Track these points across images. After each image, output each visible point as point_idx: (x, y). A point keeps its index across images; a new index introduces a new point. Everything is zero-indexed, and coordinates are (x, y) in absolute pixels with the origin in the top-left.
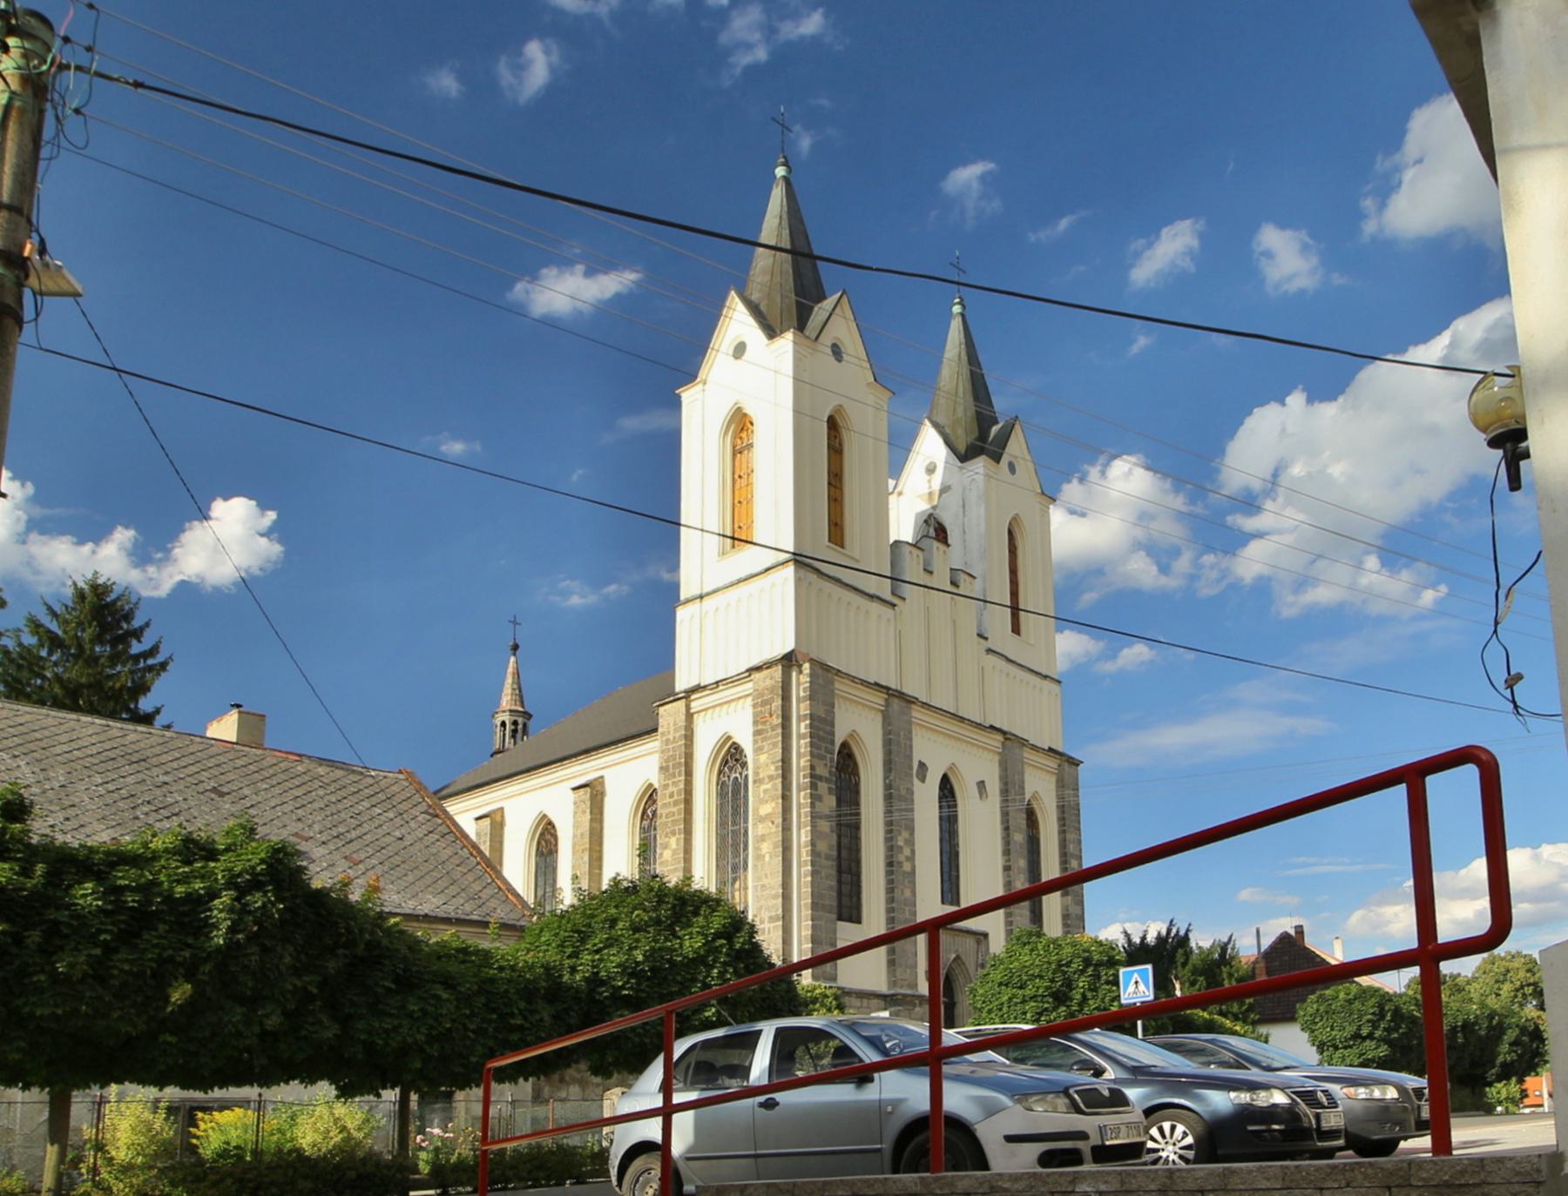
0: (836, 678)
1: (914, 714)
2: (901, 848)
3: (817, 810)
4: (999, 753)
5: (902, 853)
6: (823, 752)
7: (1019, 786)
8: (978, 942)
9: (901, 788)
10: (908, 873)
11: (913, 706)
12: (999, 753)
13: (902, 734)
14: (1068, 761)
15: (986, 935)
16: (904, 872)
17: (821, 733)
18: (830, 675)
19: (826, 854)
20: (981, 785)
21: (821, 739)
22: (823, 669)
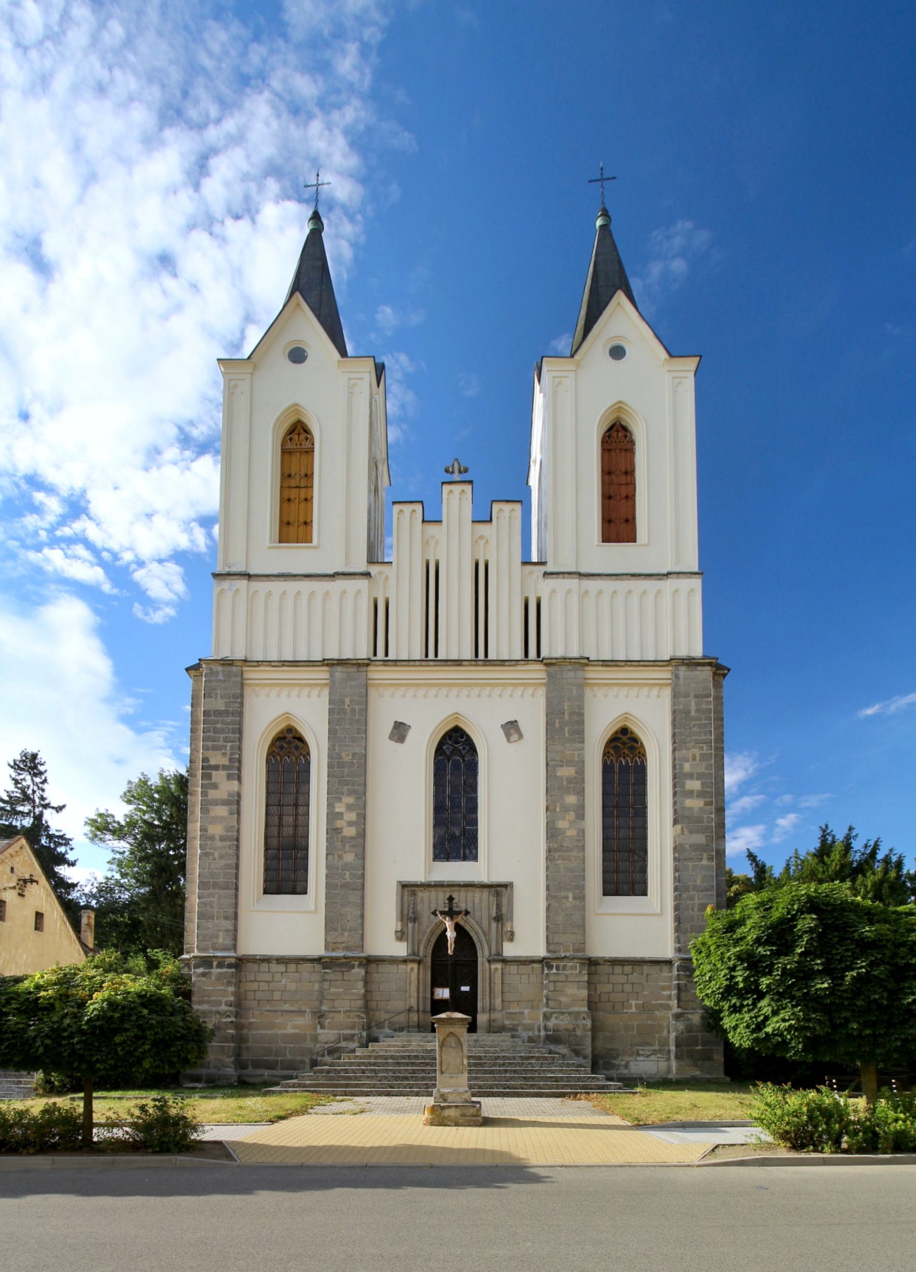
0: (245, 669)
1: (371, 675)
2: (341, 814)
3: (210, 797)
4: (544, 684)
5: (342, 819)
6: (221, 743)
7: (572, 713)
8: (498, 895)
9: (343, 755)
10: (352, 838)
11: (370, 668)
12: (544, 684)
13: (347, 701)
14: (684, 664)
15: (507, 886)
16: (345, 837)
17: (219, 726)
18: (234, 668)
19: (221, 836)
20: (511, 728)
21: (216, 731)
22: (223, 665)
